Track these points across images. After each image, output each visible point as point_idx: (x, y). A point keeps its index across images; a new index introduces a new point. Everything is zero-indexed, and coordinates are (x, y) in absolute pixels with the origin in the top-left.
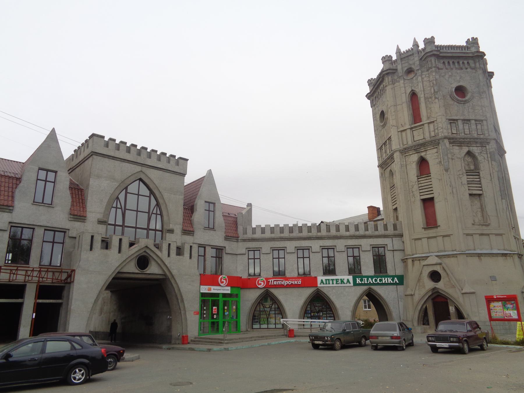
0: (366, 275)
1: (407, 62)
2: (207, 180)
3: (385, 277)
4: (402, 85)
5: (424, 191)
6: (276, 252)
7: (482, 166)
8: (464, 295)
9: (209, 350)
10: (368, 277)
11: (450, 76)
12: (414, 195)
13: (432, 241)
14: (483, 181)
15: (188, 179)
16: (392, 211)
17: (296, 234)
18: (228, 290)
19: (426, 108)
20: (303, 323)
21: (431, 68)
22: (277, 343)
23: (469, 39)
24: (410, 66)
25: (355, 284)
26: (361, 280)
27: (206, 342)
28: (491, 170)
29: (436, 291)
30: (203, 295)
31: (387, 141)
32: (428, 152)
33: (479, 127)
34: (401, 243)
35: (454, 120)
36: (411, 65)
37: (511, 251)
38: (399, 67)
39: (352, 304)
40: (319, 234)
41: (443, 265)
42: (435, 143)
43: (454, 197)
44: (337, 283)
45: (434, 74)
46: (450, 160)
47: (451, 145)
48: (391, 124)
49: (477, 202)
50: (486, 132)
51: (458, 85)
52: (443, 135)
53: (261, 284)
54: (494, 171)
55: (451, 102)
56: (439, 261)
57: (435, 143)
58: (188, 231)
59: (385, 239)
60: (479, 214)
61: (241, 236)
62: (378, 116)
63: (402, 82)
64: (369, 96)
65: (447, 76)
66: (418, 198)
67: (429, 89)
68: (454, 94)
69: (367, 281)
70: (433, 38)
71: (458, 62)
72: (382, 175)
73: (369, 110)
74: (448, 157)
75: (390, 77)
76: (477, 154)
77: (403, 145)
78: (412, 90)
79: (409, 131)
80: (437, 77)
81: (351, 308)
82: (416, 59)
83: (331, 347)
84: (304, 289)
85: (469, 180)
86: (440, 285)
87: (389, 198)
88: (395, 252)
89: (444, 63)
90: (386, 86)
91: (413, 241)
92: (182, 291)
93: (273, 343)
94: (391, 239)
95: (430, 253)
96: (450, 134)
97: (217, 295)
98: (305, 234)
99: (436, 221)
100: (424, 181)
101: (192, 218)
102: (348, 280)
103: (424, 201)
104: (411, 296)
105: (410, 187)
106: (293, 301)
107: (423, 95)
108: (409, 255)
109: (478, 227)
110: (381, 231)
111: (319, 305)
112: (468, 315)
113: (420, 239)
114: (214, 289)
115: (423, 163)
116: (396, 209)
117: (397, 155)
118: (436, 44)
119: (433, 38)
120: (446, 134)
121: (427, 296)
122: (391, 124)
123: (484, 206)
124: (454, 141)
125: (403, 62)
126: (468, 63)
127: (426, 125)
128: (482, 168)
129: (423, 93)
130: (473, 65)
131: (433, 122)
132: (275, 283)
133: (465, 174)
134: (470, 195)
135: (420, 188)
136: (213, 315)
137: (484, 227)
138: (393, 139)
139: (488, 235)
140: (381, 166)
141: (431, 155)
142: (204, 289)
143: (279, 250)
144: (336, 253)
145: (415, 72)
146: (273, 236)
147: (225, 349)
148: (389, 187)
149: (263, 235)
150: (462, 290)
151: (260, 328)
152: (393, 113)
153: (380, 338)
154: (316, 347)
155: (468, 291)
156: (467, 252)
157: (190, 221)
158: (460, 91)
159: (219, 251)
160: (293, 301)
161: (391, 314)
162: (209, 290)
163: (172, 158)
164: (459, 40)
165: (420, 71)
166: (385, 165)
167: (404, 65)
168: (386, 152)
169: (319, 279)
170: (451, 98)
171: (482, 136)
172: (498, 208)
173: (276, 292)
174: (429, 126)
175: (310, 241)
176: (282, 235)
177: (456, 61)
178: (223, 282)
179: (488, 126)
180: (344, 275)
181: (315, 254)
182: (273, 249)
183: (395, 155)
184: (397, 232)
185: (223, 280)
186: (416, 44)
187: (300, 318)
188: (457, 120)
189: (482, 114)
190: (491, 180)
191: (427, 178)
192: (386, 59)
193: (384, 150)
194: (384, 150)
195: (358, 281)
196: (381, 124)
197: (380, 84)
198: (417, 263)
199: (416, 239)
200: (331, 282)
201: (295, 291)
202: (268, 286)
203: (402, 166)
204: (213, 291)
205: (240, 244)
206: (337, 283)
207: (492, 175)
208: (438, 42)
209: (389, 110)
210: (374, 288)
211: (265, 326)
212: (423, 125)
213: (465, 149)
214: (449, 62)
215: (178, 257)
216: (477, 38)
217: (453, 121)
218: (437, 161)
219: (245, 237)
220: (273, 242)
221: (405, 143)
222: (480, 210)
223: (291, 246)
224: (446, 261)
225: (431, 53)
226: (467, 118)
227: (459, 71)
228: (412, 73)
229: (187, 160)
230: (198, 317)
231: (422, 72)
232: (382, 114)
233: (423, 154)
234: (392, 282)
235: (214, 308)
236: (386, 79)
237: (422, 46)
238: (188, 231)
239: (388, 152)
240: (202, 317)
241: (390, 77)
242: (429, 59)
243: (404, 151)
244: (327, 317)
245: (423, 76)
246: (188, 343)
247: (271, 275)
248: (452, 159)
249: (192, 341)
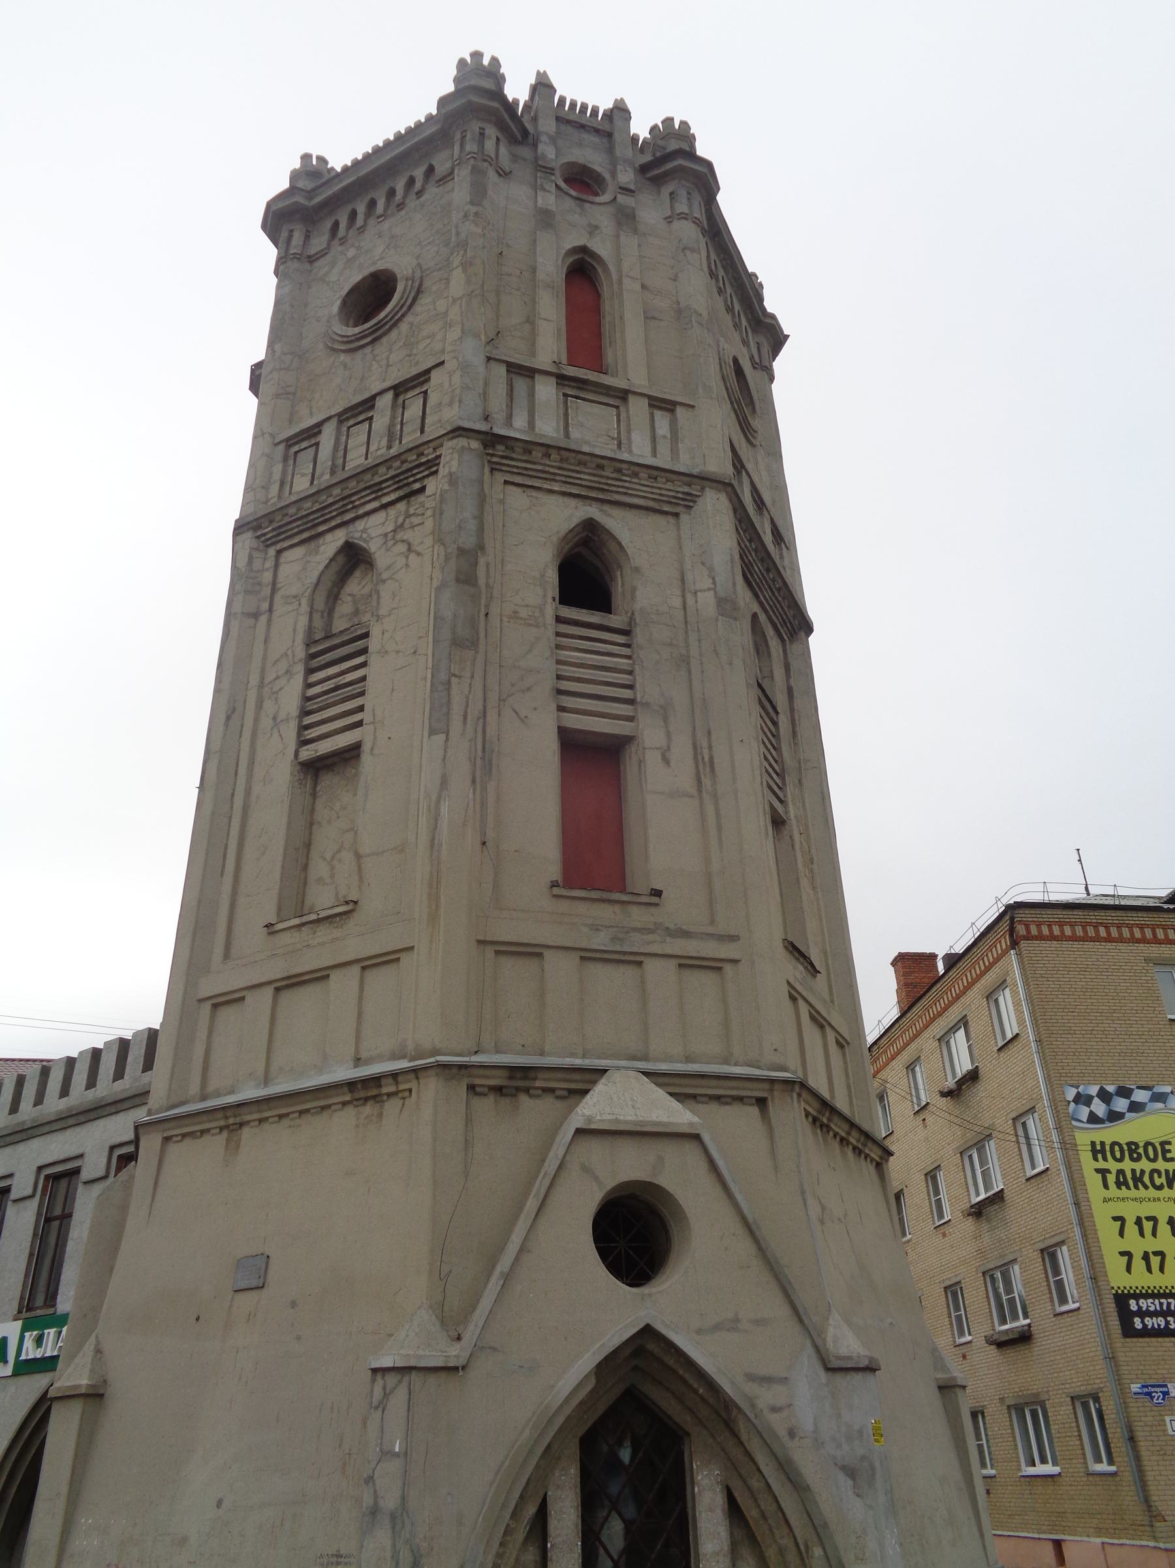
33: (414, 410)
47: (272, 552)
69: (53, 1349)
133: (300, 669)
213: (332, 543)
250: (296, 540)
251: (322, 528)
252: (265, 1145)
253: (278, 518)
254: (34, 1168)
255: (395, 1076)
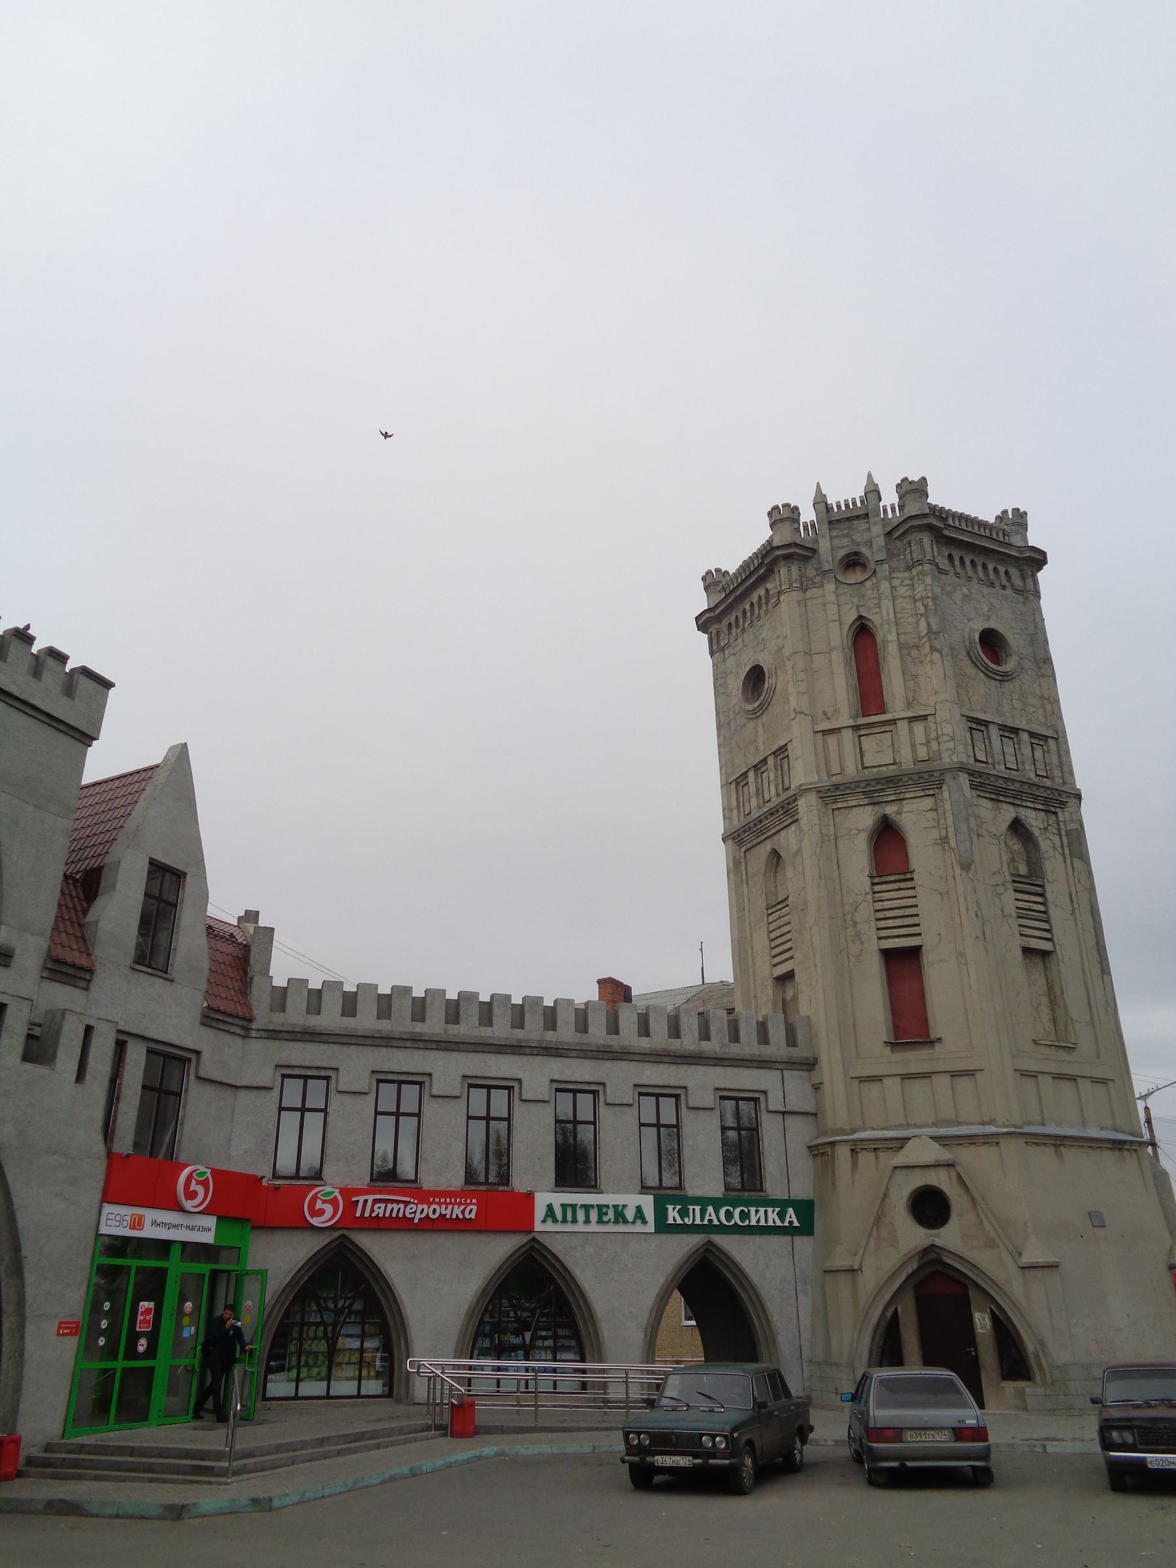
0: (699, 1193)
1: (847, 535)
2: (168, 782)
3: (759, 1203)
4: (831, 597)
5: (891, 923)
6: (388, 1090)
7: (1048, 866)
8: (1026, 1271)
9: (176, 1512)
10: (703, 1202)
11: (967, 598)
12: (858, 935)
13: (916, 1087)
14: (1053, 913)
15: (101, 763)
16: (770, 982)
17: (468, 1028)
18: (205, 1230)
19: (904, 673)
20: (466, 1374)
21: (920, 562)
22: (439, 1463)
23: (1005, 512)
24: (855, 549)
25: (662, 1227)
26: (683, 1213)
27: (118, 1467)
28: (1072, 883)
29: (933, 1256)
30: (119, 1246)
31: (771, 761)
32: (908, 806)
33: (1038, 753)
34: (809, 1090)
35: (979, 722)
36: (858, 544)
37: (1132, 1134)
38: (824, 546)
39: (649, 1300)
40: (550, 1036)
41: (959, 1168)
42: (929, 779)
43: (987, 951)
44: (600, 1221)
45: (928, 580)
46: (975, 837)
48: (793, 704)
49: (1038, 975)
50: (1057, 773)
51: (986, 626)
52: (955, 760)
53: (321, 1212)
54: (1080, 888)
55: (971, 671)
56: (945, 1155)
57: (929, 779)
58: (73, 966)
59: (762, 1071)
60: (1045, 1013)
61: (263, 1016)
62: (736, 683)
63: (830, 587)
64: (704, 623)
65: (958, 596)
66: (872, 947)
67: (911, 620)
68: (979, 646)
69: (702, 1219)
70: (924, 479)
71: (984, 566)
72: (737, 869)
73: (705, 663)
74: (969, 828)
75: (794, 569)
76: (1036, 833)
77: (828, 772)
78: (861, 617)
79: (848, 735)
80: (938, 590)
81: (644, 1318)
82: (877, 530)
83: (712, 1480)
84: (484, 1238)
85: (1020, 904)
86: (949, 1237)
87: (761, 941)
88: (790, 1119)
89: (950, 557)
90: (779, 593)
91: (856, 1082)
92: (20, 1226)
93: (428, 1466)
94: (778, 1073)
95: (908, 1126)
96: (972, 761)
97: (163, 1247)
98: (501, 1030)
99: (924, 1022)
100: (892, 895)
101: (90, 917)
102: (639, 1210)
103: (889, 955)
104: (848, 1276)
105: (847, 908)
106: (437, 1286)
107: (892, 637)
108: (842, 1131)
109: (1047, 1051)
110: (749, 1045)
111: (534, 1305)
112: (1042, 1343)
113: (878, 1079)
114: (157, 1224)
115: (887, 839)
116: (789, 976)
117: (807, 806)
118: (932, 500)
119: (924, 479)
120: (964, 760)
121: (903, 1277)
122: (793, 704)
123: (1057, 991)
124: (986, 784)
125: (834, 533)
126: (1006, 572)
127: (903, 725)
128: (1050, 877)
129: (894, 629)
130: (1018, 583)
131: (925, 718)
132: (379, 1210)
133: (1010, 886)
134: (1027, 951)
135: (880, 915)
136: (134, 1337)
137: (1062, 1054)
138: (794, 751)
139: (1073, 1079)
140: (734, 837)
141: (914, 817)
142: (117, 1221)
143: (400, 1083)
144: (603, 1110)
145: (872, 566)
146: (385, 1026)
147: (256, 1501)
148: (761, 903)
149: (349, 1023)
150: (1020, 1254)
151: (296, 1397)
152: (802, 676)
153: (909, 1436)
154: (644, 1478)
155: (1041, 1260)
156: (1026, 1129)
157: (81, 926)
158: (991, 643)
159: (169, 1068)
160: (437, 1286)
161: (772, 1339)
162: (133, 1227)
163: (50, 662)
164: (984, 507)
165: (886, 566)
166: (754, 835)
167: (836, 542)
168: (759, 792)
169: (542, 1200)
170: (970, 658)
171: (1048, 783)
172: (1092, 999)
173: (373, 1245)
174: (911, 729)
175: (517, 1058)
176: (419, 1028)
177: (979, 561)
178: (191, 1195)
179: (1060, 757)
180: (626, 1191)
181: (531, 1106)
182: (381, 1078)
183: (802, 803)
184: (798, 1053)
185: (194, 1186)
186: (873, 492)
187: (459, 1354)
188: (986, 724)
189: (1042, 719)
190: (1073, 913)
191: (902, 885)
192: (782, 516)
193: (752, 787)
194: (752, 787)
195: (673, 1214)
196: (750, 707)
197: (754, 586)
198: (866, 1158)
199: (864, 1080)
200: (581, 1215)
201: (452, 1244)
202: (351, 1221)
203: (824, 839)
204: (149, 1232)
205: (256, 1046)
206: (600, 1221)
207: (1074, 897)
208: (937, 497)
209: (789, 665)
210: (725, 1242)
211: (311, 1388)
212: (894, 722)
213: (1008, 814)
214: (961, 559)
215: (28, 1066)
216: (1025, 513)
217: (977, 725)
218: (935, 834)
219: (279, 1020)
220: (384, 1051)
221: (835, 769)
222: (1044, 1000)
223: (447, 1070)
224: (965, 1156)
225: (925, 521)
226: (1010, 723)
227: (985, 590)
228: (859, 569)
229: (108, 685)
230: (71, 1344)
231: (893, 570)
232: (756, 678)
233: (890, 810)
234: (779, 1223)
235: (145, 1305)
236: (784, 571)
237: (890, 498)
238: (69, 967)
239: (771, 792)
240: (89, 1347)
241: (794, 569)
242: (917, 536)
243: (833, 795)
244: (555, 1350)
245: (896, 582)
246: (19, 1474)
247: (360, 1177)
248: (979, 835)
249: (30, 1461)
250: (988, 795)
251: (1002, 798)
252: (1072, 1156)
253: (984, 777)
254: (631, 1085)
255: (1132, 1142)
